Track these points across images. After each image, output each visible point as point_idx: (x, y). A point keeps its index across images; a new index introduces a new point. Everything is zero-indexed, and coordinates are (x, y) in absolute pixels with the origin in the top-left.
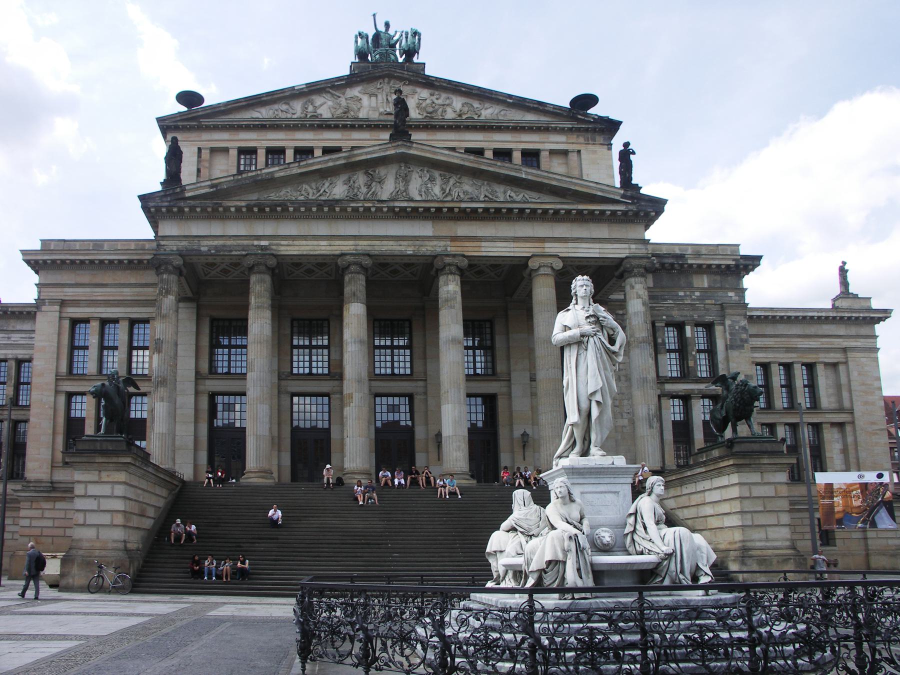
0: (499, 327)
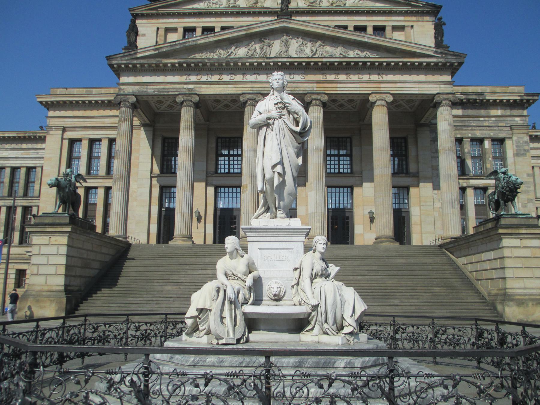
0: (355, 142)
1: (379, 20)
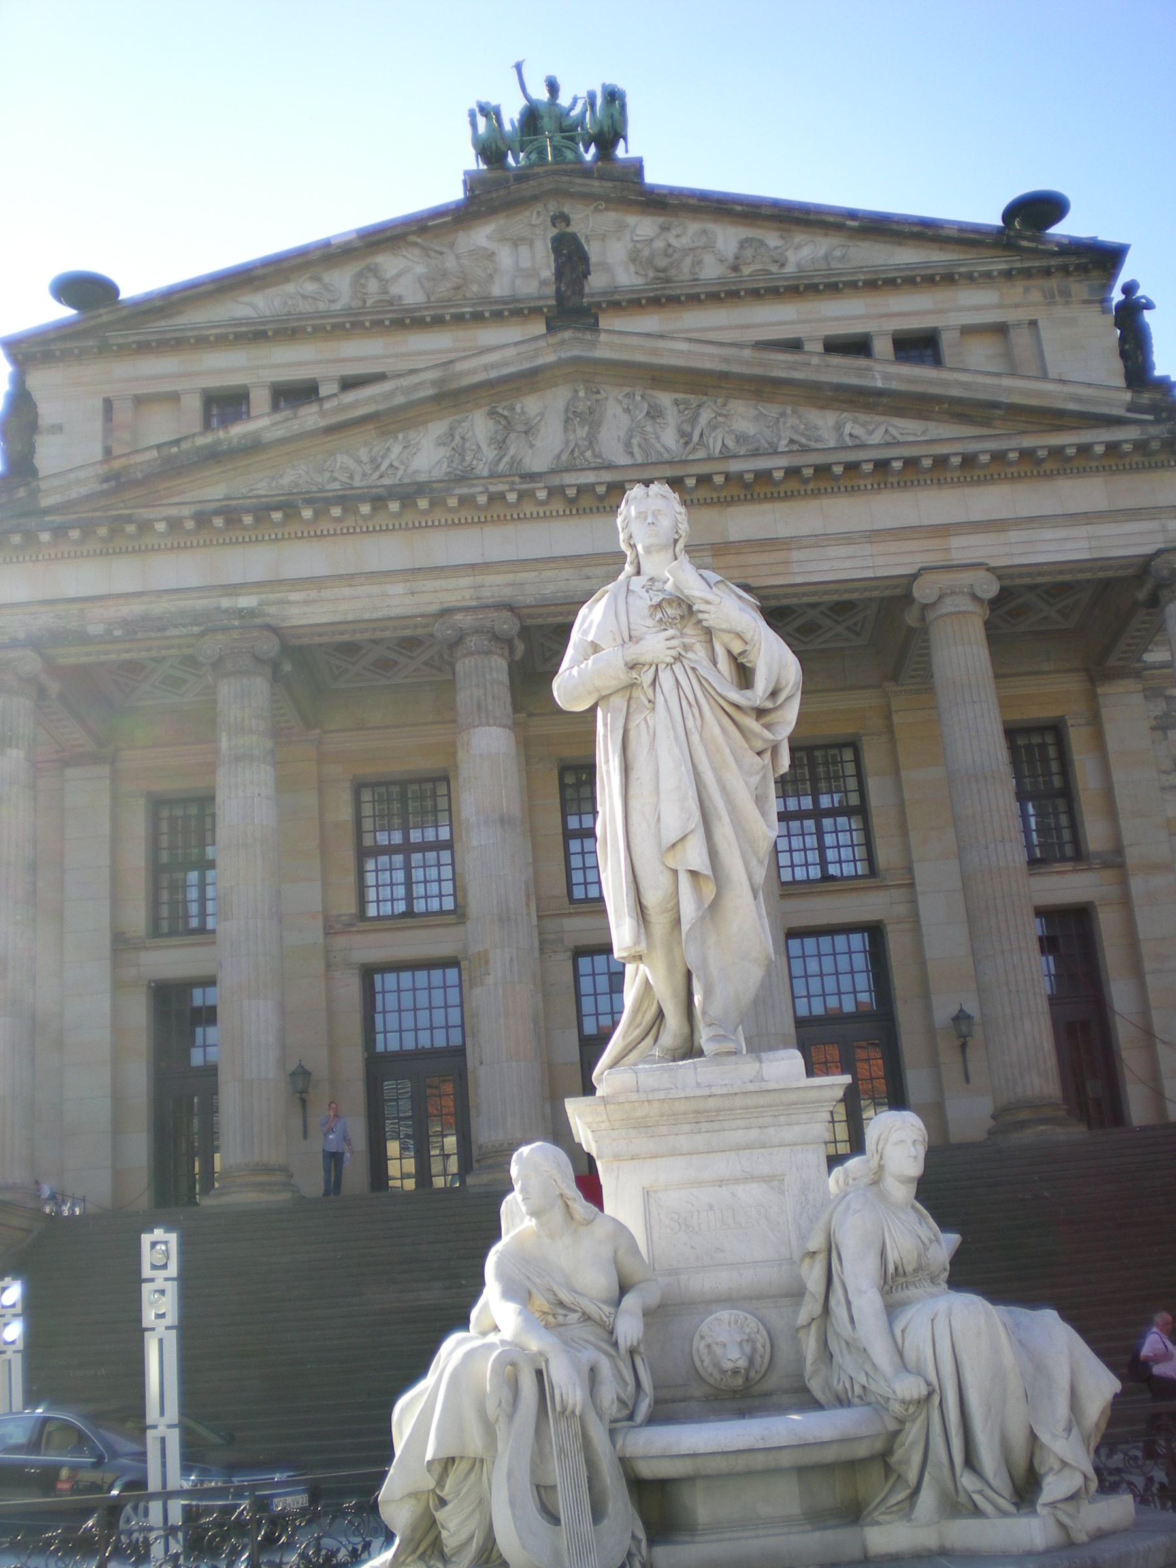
0: (873, 757)
1: (912, 310)
